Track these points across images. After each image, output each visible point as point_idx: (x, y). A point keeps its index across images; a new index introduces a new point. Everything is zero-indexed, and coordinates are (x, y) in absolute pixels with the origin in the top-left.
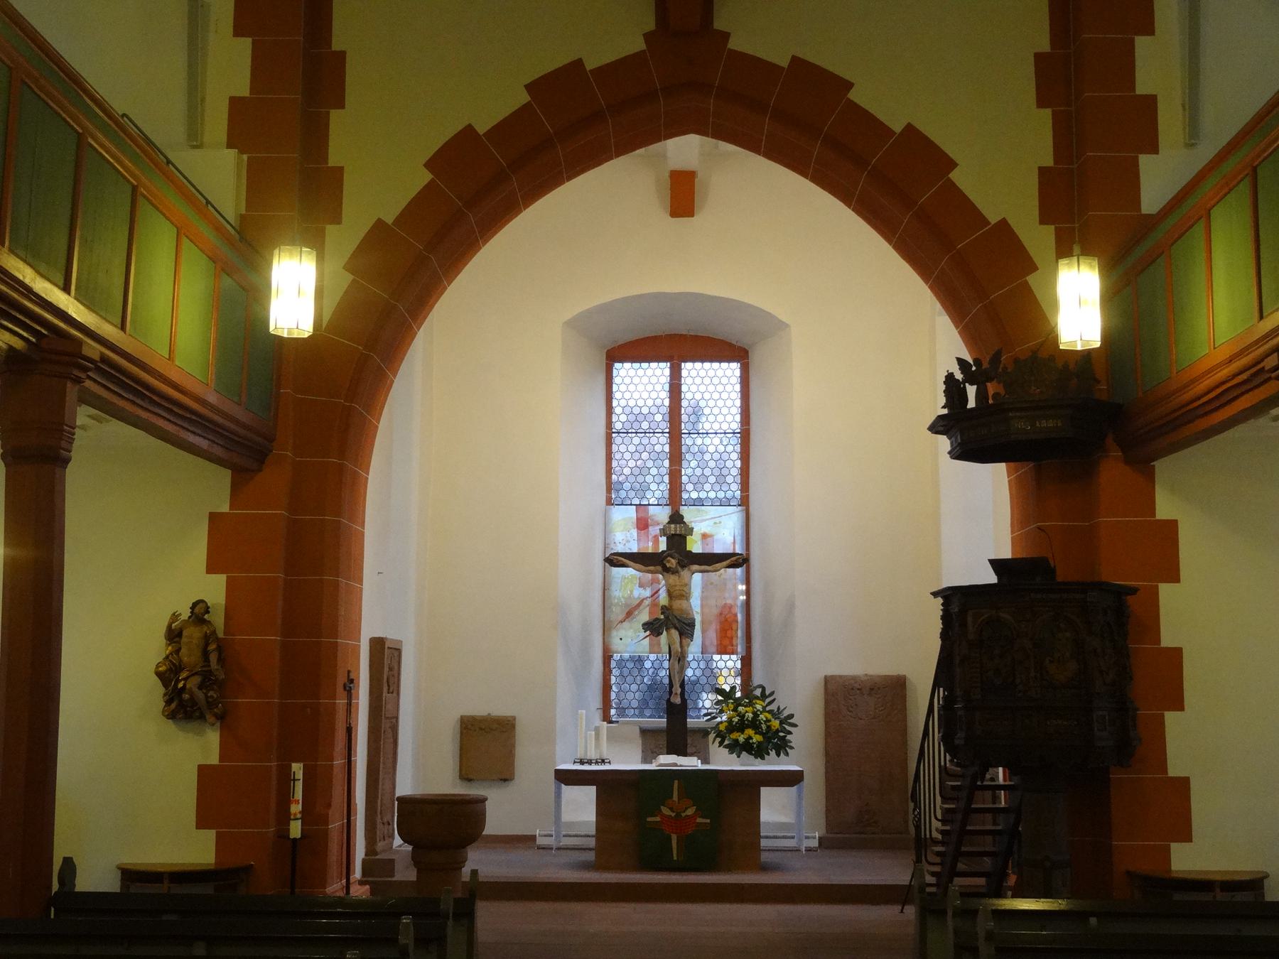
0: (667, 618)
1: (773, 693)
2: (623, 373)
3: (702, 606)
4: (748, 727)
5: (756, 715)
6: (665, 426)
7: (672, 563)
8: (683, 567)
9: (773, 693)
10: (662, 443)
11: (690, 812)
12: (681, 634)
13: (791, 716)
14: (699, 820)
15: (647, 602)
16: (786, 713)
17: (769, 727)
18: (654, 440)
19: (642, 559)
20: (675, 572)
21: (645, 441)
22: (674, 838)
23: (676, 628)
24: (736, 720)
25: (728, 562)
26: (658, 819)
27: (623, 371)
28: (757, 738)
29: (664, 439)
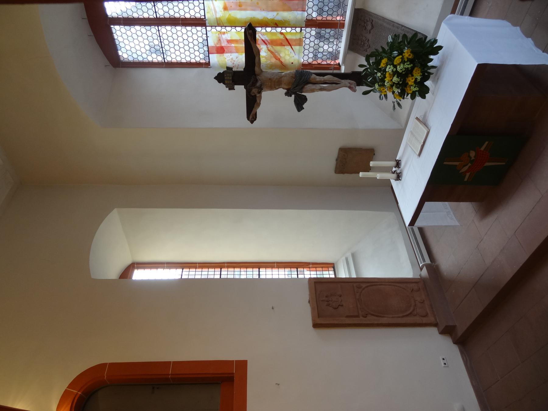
2: (125, 56)
3: (273, 10)
6: (154, 29)
10: (165, 30)
11: (473, 154)
14: (482, 149)
15: (270, 47)
17: (409, 60)
18: (165, 36)
21: (166, 42)
22: (487, 164)
25: (252, 43)
26: (468, 175)
27: (125, 54)
28: (417, 75)
29: (163, 29)
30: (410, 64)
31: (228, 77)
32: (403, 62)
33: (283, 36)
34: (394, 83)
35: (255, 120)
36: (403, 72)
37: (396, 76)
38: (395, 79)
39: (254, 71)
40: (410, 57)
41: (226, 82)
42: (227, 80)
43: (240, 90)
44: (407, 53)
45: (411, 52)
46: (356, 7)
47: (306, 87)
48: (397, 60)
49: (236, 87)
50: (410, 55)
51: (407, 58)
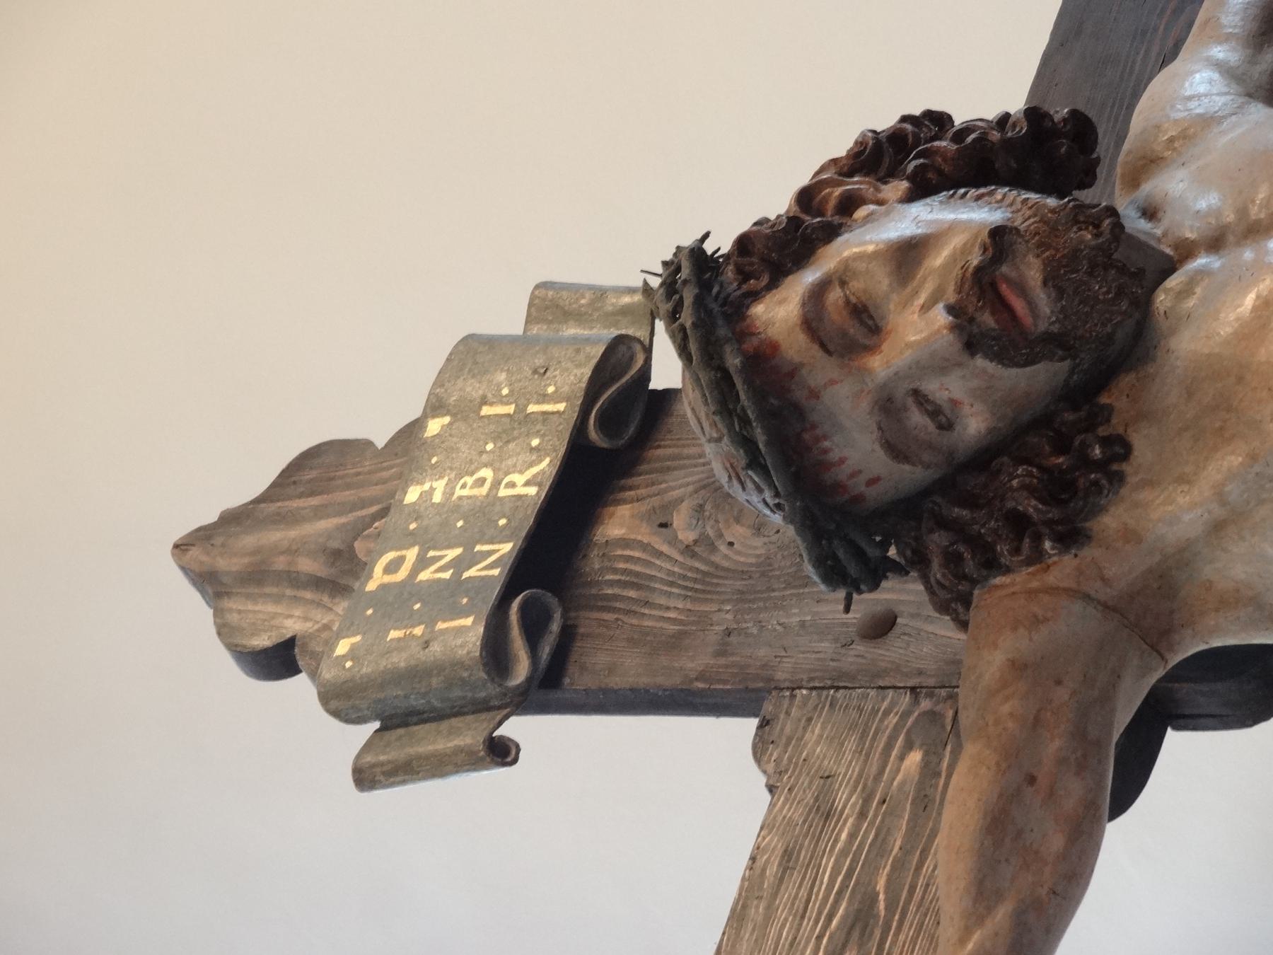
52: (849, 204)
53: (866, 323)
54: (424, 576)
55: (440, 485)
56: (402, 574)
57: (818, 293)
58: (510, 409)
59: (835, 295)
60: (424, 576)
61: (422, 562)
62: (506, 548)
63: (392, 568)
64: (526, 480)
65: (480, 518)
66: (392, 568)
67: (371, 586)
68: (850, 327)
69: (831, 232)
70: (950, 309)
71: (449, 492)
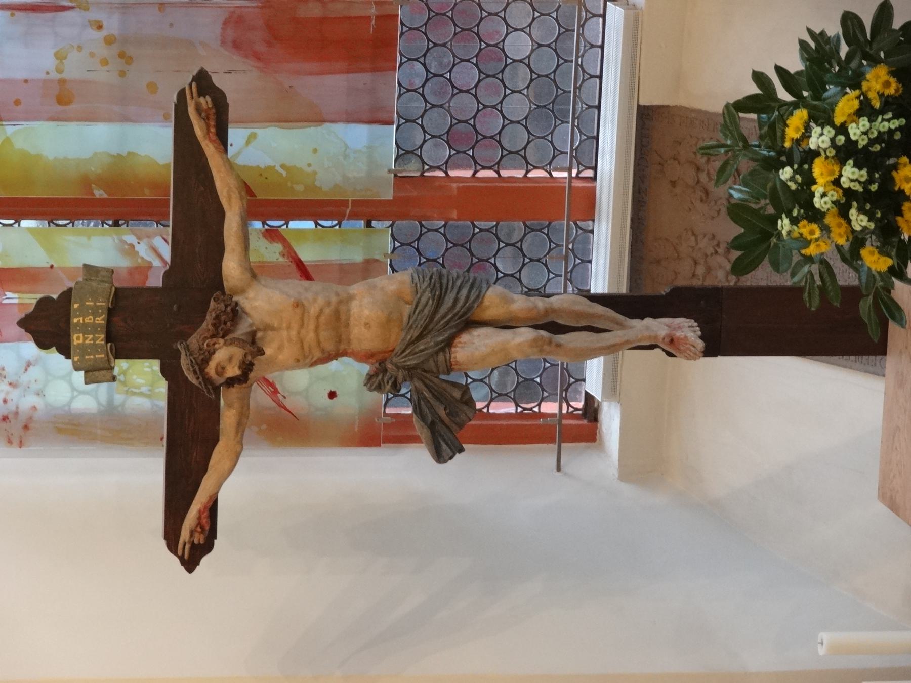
0: (411, 372)
1: (759, 78)
4: (887, 181)
5: (846, 152)
7: (225, 358)
8: (235, 313)
9: (759, 78)
12: (470, 323)
13: (849, 20)
16: (834, 29)
17: (888, 103)
19: (189, 449)
20: (253, 345)
23: (449, 343)
24: (859, 221)
25: (209, 149)
30: (896, 117)
31: (88, 324)
32: (865, 110)
33: (278, 247)
34: (849, 193)
35: (207, 547)
36: (872, 142)
37: (851, 162)
38: (850, 174)
39: (216, 282)
40: (891, 91)
41: (77, 339)
42: (85, 329)
43: (143, 384)
44: (878, 81)
45: (892, 74)
46: (643, 102)
47: (465, 337)
48: (846, 105)
49: (121, 365)
50: (887, 84)
51: (881, 95)
52: (214, 344)
53: (223, 368)
54: (87, 342)
55: (81, 319)
56: (81, 341)
57: (217, 366)
58: (92, 303)
59: (220, 369)
60: (87, 342)
61: (85, 339)
62: (103, 336)
63: (78, 338)
64: (101, 320)
65: (94, 329)
66: (78, 338)
67: (75, 343)
68: (221, 370)
69: (214, 353)
70: (240, 368)
71: (84, 320)
